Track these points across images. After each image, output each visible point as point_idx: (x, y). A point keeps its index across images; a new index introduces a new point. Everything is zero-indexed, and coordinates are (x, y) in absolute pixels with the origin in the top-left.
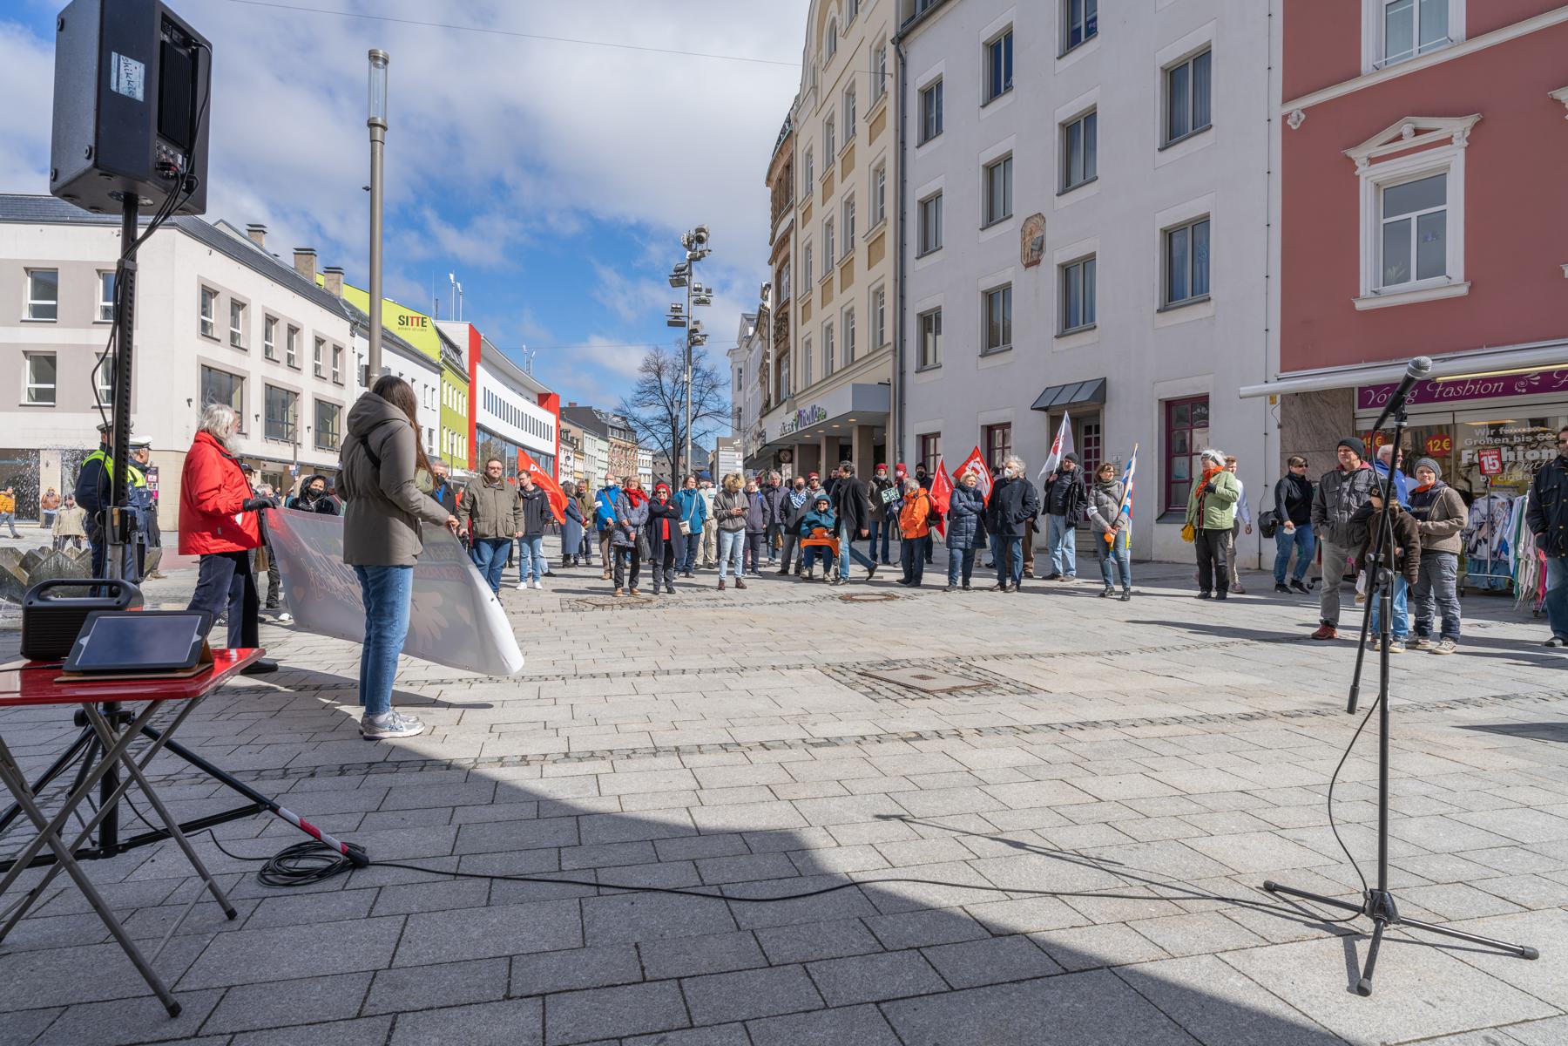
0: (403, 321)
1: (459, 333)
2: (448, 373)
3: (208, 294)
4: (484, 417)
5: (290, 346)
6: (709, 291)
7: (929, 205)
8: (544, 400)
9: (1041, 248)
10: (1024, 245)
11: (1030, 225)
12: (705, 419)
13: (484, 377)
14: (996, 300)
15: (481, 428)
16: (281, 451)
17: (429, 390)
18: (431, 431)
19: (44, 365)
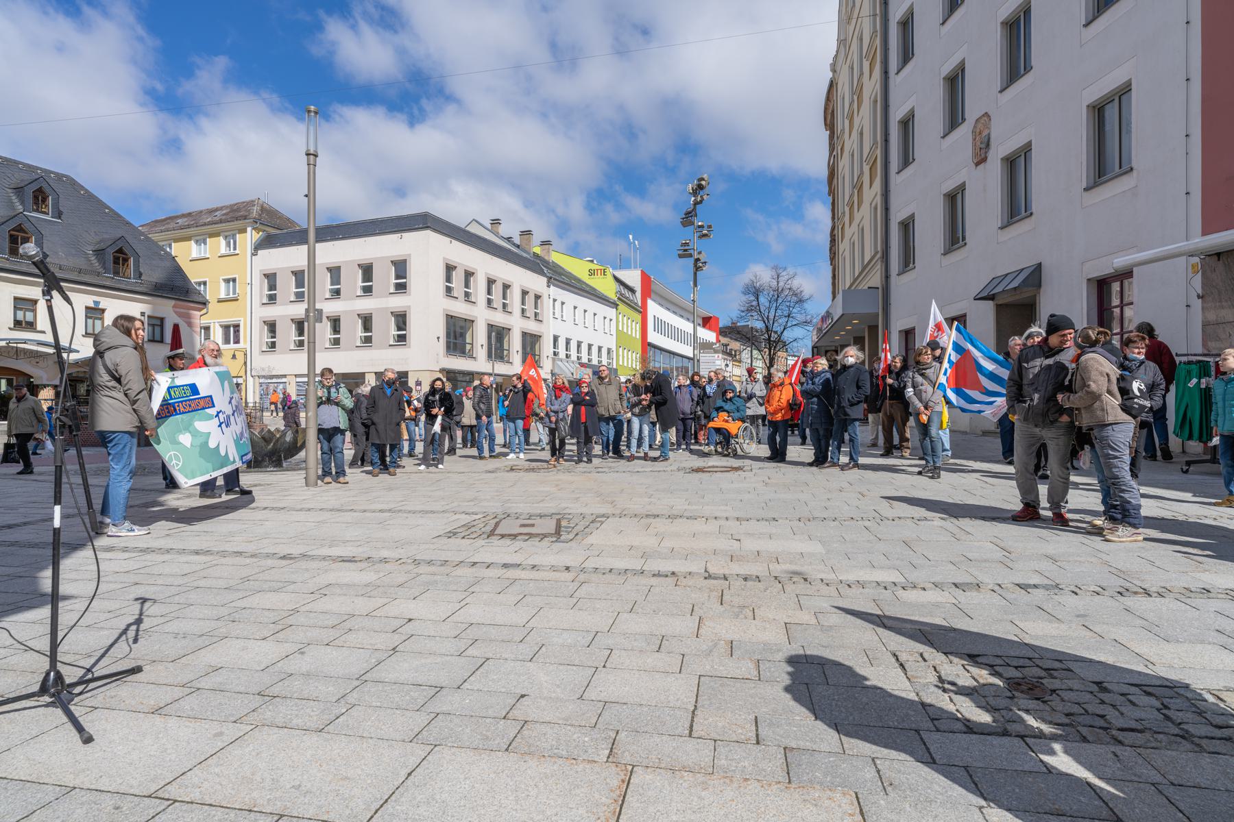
0: (592, 273)
1: (633, 277)
2: (622, 307)
3: (450, 269)
4: (654, 337)
5: (504, 297)
6: (710, 227)
7: (907, 124)
8: (707, 322)
9: (988, 145)
10: (974, 145)
11: (980, 126)
12: (795, 328)
13: (653, 308)
14: (954, 199)
15: (650, 344)
16: (501, 368)
17: (607, 321)
18: (609, 350)
19: (367, 322)
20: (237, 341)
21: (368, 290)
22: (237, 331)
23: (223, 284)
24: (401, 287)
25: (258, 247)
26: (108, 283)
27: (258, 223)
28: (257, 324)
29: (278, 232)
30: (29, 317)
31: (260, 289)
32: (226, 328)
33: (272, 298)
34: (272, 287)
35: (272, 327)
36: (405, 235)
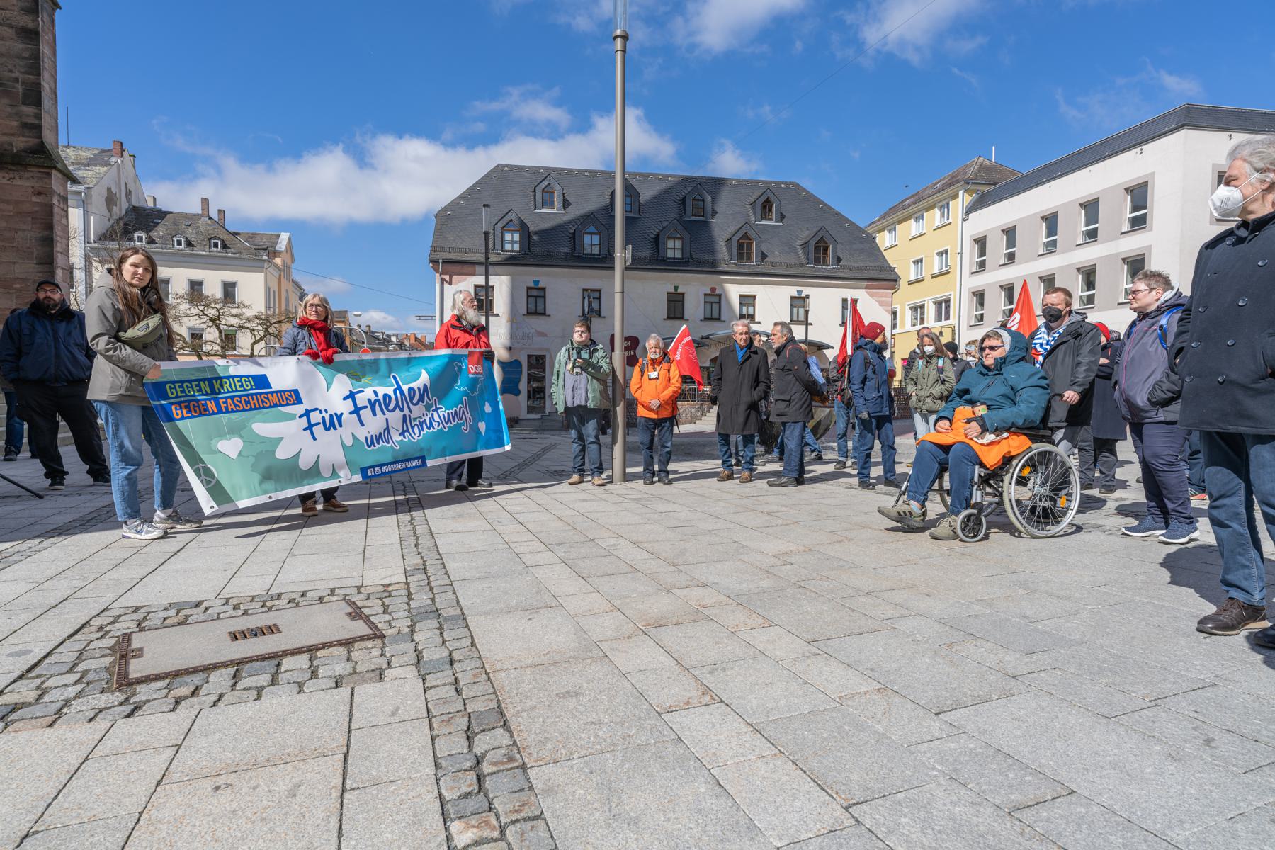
20: (947, 318)
21: (1092, 235)
22: (948, 307)
23: (937, 258)
24: (1139, 223)
25: (970, 210)
26: (808, 273)
27: (970, 184)
28: (966, 295)
29: (992, 187)
30: (751, 312)
31: (970, 255)
32: (938, 304)
33: (982, 265)
34: (982, 252)
35: (980, 296)
36: (1147, 148)
